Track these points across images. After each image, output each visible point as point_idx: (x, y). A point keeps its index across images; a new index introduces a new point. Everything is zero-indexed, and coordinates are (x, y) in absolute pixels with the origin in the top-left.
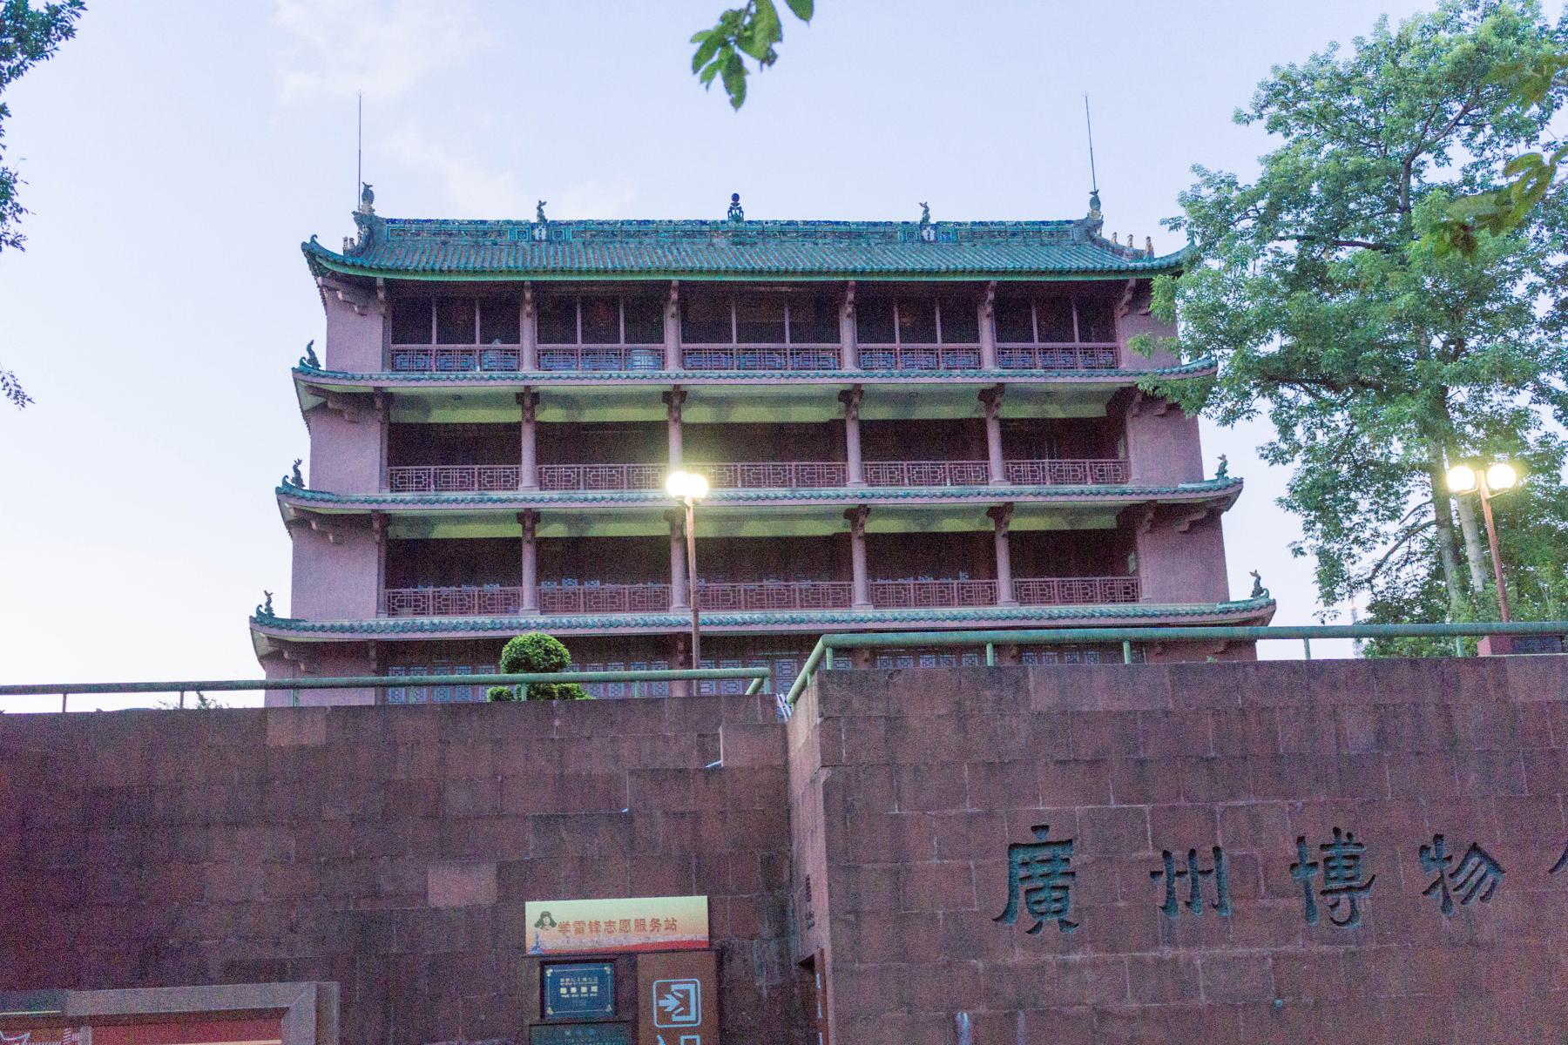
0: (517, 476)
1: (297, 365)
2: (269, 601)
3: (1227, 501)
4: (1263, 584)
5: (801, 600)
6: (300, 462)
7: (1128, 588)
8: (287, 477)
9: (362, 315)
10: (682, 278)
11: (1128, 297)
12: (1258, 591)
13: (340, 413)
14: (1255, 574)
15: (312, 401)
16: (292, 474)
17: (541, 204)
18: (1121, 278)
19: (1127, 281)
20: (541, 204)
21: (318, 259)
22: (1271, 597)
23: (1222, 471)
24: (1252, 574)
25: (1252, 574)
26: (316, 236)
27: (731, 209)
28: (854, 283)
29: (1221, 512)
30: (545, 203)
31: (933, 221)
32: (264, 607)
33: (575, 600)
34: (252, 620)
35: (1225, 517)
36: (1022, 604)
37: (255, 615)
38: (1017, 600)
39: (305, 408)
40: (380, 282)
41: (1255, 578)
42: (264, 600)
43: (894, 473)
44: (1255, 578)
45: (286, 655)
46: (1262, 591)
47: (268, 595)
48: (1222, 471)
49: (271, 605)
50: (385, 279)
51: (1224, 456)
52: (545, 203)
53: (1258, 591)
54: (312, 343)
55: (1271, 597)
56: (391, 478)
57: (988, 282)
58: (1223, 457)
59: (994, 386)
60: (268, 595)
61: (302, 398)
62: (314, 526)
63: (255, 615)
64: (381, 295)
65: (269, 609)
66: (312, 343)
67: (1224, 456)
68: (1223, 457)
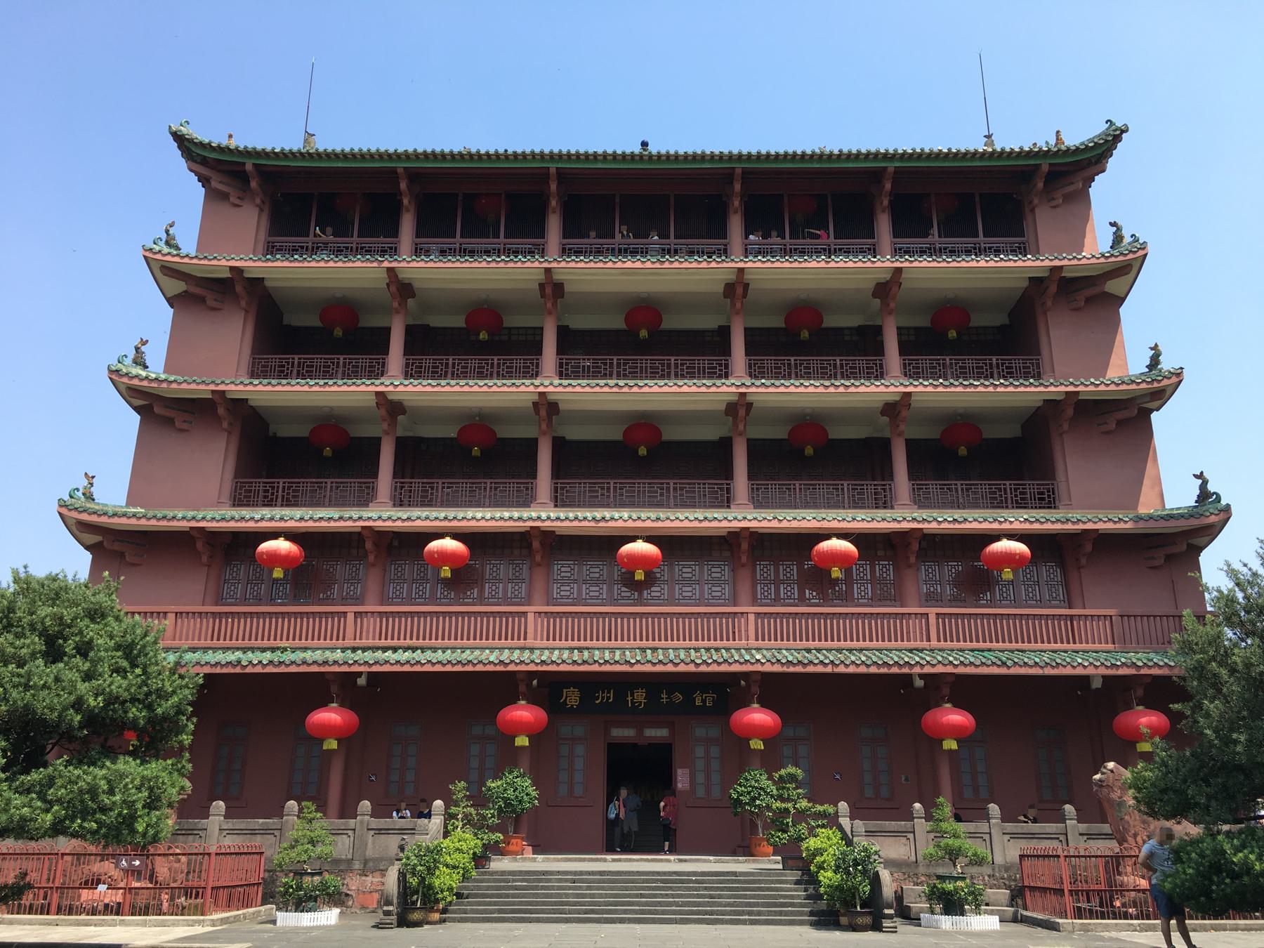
0: (383, 366)
1: (150, 245)
3: (1160, 396)
4: (1211, 488)
6: (144, 343)
7: (1042, 493)
8: (126, 356)
10: (560, 165)
11: (1040, 185)
12: (1205, 495)
13: (201, 300)
14: (1200, 476)
15: (179, 287)
18: (1032, 162)
19: (1038, 166)
21: (186, 143)
22: (1223, 502)
23: (1155, 362)
24: (1195, 476)
25: (1195, 476)
28: (739, 171)
29: (1151, 411)
33: (432, 494)
34: (62, 504)
35: (1155, 416)
36: (920, 507)
38: (916, 504)
39: (169, 295)
40: (249, 167)
41: (1200, 481)
43: (780, 368)
44: (1200, 481)
45: (105, 543)
46: (1209, 495)
47: (90, 479)
48: (1155, 362)
50: (254, 165)
51: (1156, 345)
53: (1205, 495)
55: (1223, 502)
57: (887, 167)
58: (1155, 348)
59: (888, 276)
60: (90, 479)
62: (156, 410)
63: (66, 498)
64: (253, 184)
65: (90, 497)
67: (1156, 345)
68: (1155, 348)
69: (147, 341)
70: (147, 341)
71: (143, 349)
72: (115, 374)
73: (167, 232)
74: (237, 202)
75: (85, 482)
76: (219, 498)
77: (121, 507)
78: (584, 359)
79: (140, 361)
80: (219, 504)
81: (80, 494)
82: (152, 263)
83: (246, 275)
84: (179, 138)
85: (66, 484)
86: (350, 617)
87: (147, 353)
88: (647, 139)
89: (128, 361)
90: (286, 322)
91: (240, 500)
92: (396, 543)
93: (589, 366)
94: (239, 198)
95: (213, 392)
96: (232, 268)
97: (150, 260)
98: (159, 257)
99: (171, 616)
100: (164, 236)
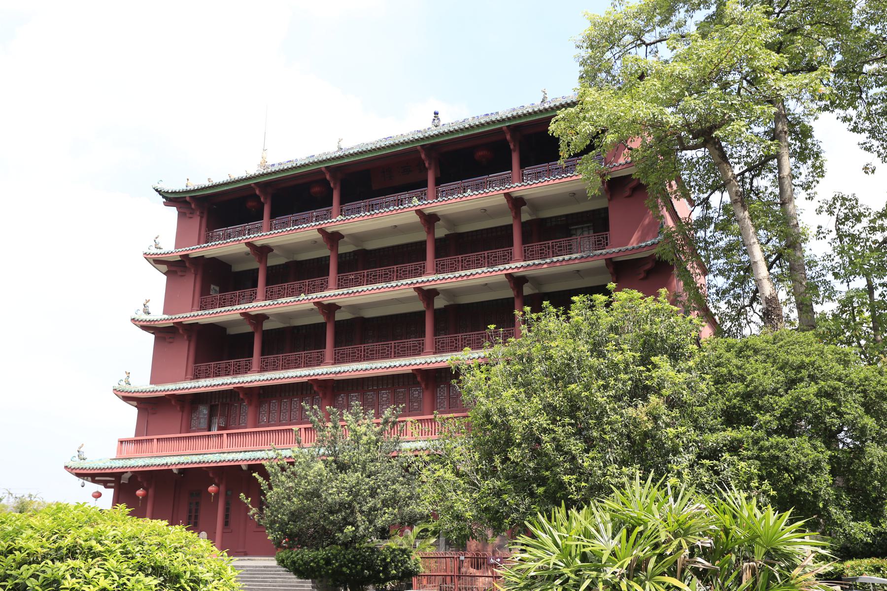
5: (395, 354)
6: (148, 301)
27: (434, 120)
31: (549, 99)
40: (188, 199)
71: (148, 304)
74: (191, 216)
76: (186, 375)
80: (185, 379)
81: (123, 383)
83: (191, 256)
84: (159, 191)
85: (116, 380)
86: (225, 436)
88: (437, 110)
91: (196, 376)
92: (261, 392)
96: (181, 256)
98: (149, 256)
99: (155, 441)
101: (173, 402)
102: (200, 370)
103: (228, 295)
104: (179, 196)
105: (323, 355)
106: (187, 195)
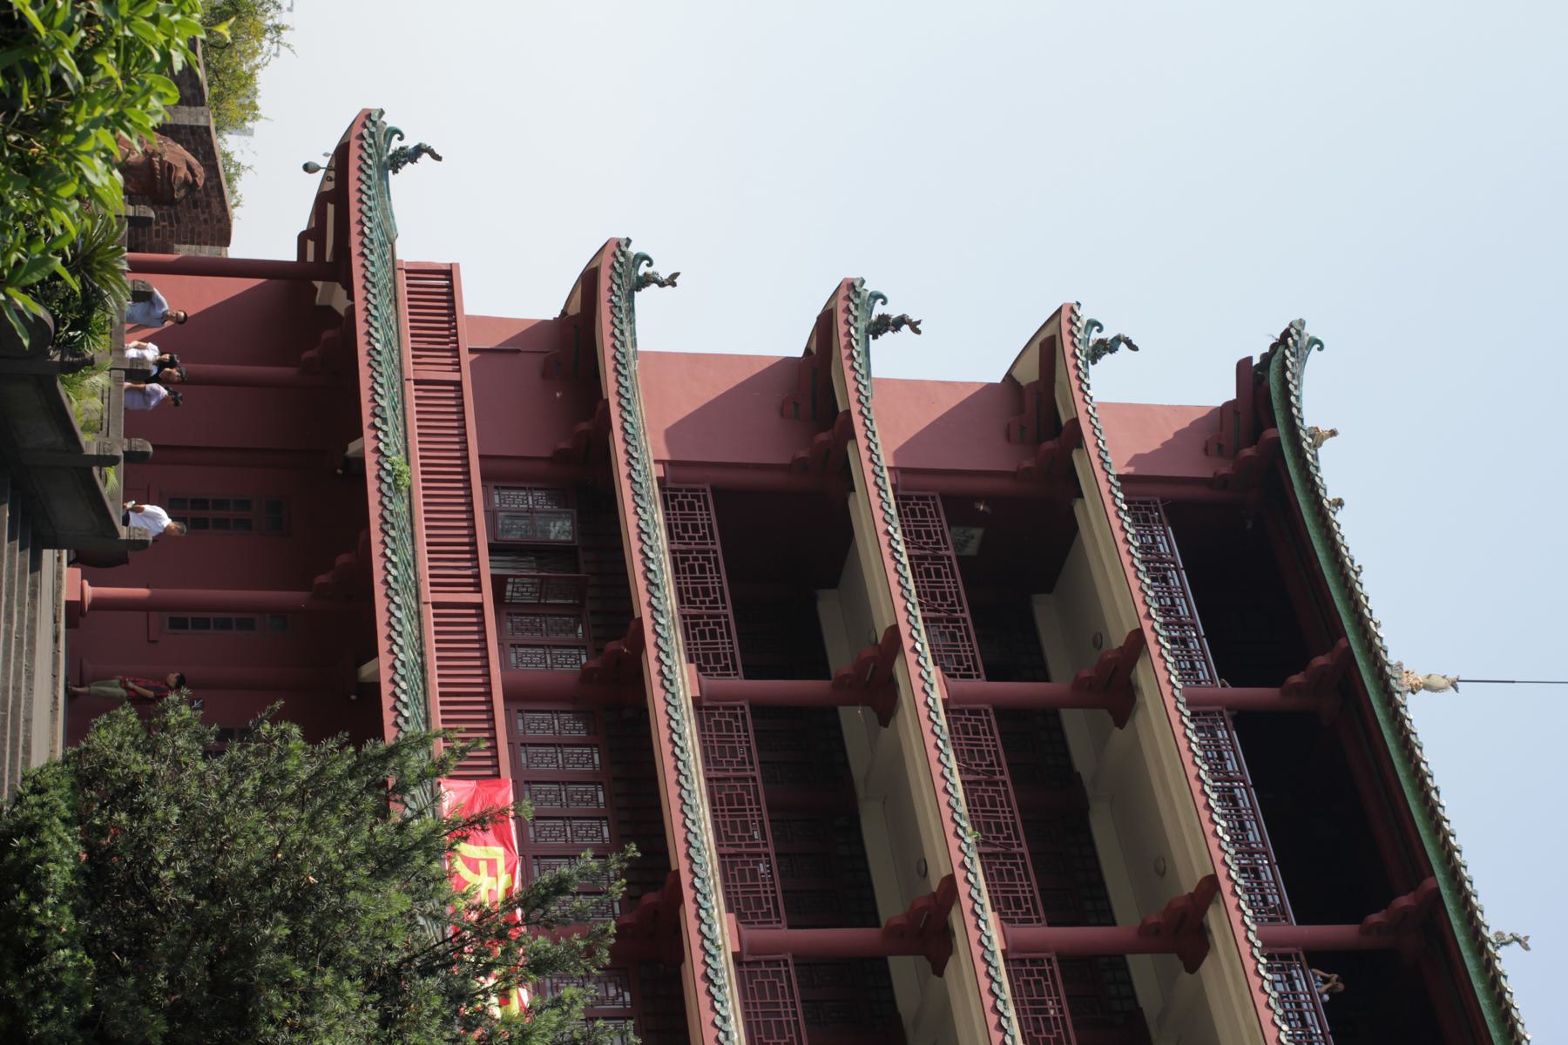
1: (1085, 314)
2: (662, 284)
9: (1206, 451)
16: (893, 311)
17: (1523, 942)
20: (1523, 942)
26: (1321, 348)
30: (1527, 948)
32: (650, 270)
37: (633, 250)
39: (1014, 374)
40: (1269, 434)
42: (663, 271)
47: (672, 281)
49: (654, 286)
50: (1277, 440)
52: (1527, 948)
54: (1133, 347)
56: (918, 498)
61: (1028, 352)
66: (1133, 347)
69: (918, 332)
70: (918, 332)
71: (905, 328)
72: (850, 289)
73: (1118, 339)
75: (664, 275)
77: (634, 343)
78: (1059, 1002)
79: (884, 325)
81: (643, 269)
82: (1054, 324)
83: (1075, 455)
87: (897, 334)
89: (879, 309)
90: (1036, 598)
91: (670, 493)
93: (1046, 1011)
94: (1220, 446)
95: (848, 413)
96: (1075, 422)
97: (1057, 320)
98: (1066, 327)
100: (1108, 334)
101: (584, 426)
102: (691, 506)
103: (954, 584)
104: (1276, 404)
105: (766, 921)
106: (1281, 431)
